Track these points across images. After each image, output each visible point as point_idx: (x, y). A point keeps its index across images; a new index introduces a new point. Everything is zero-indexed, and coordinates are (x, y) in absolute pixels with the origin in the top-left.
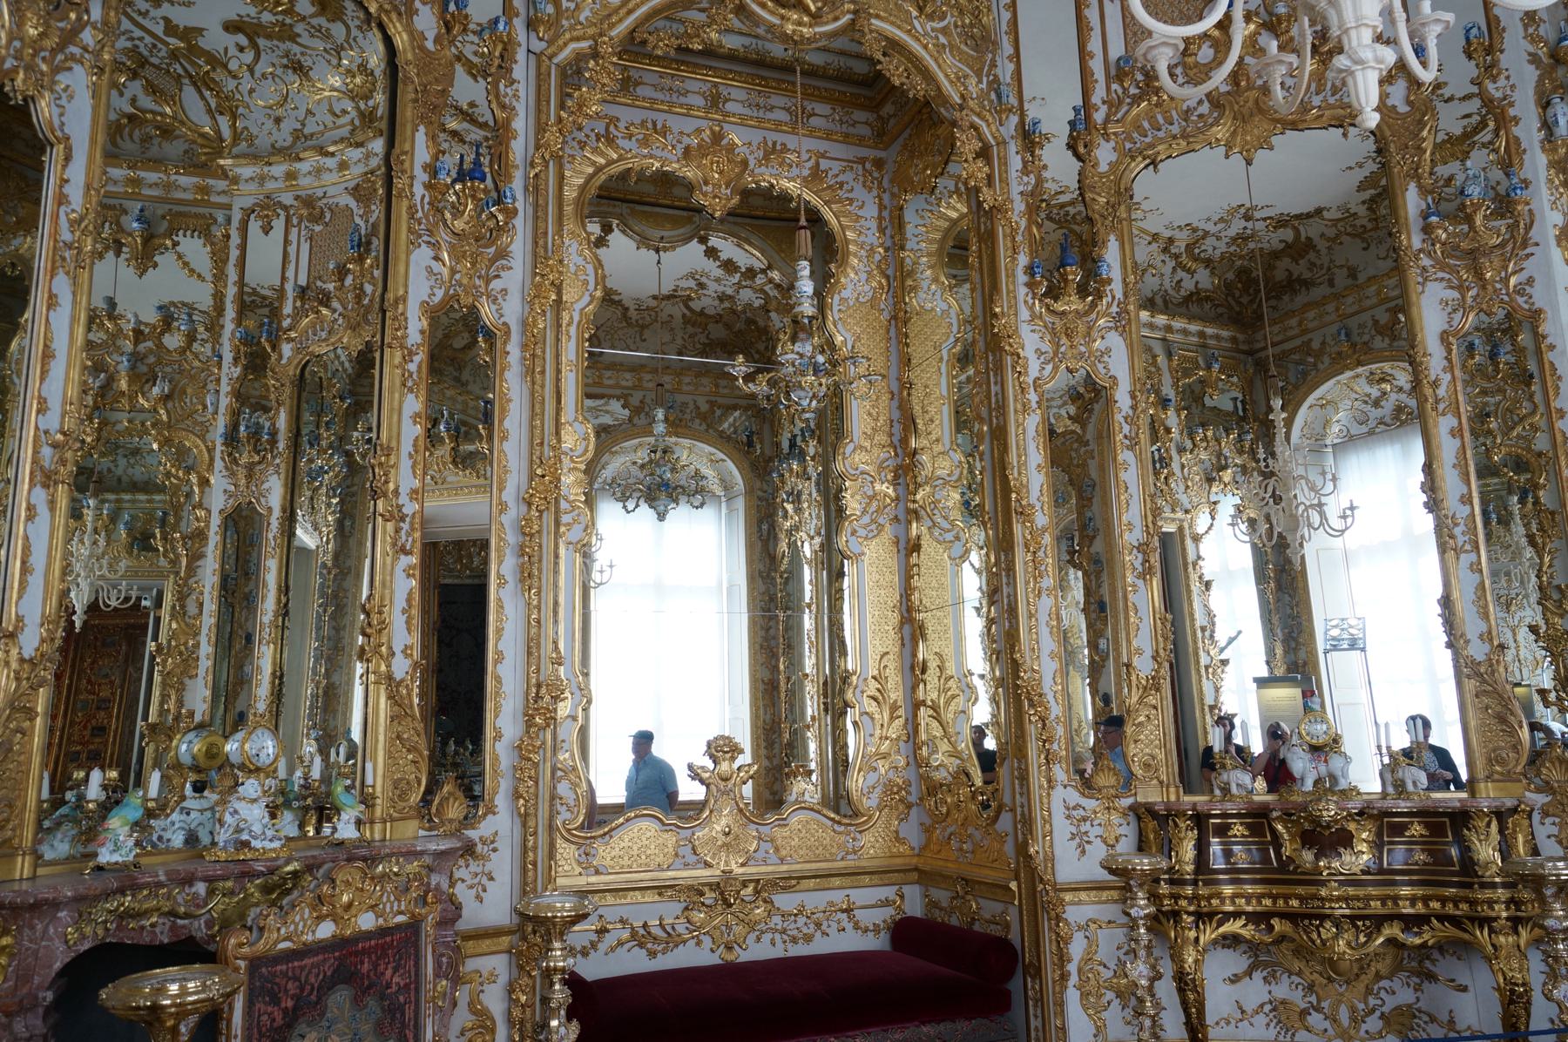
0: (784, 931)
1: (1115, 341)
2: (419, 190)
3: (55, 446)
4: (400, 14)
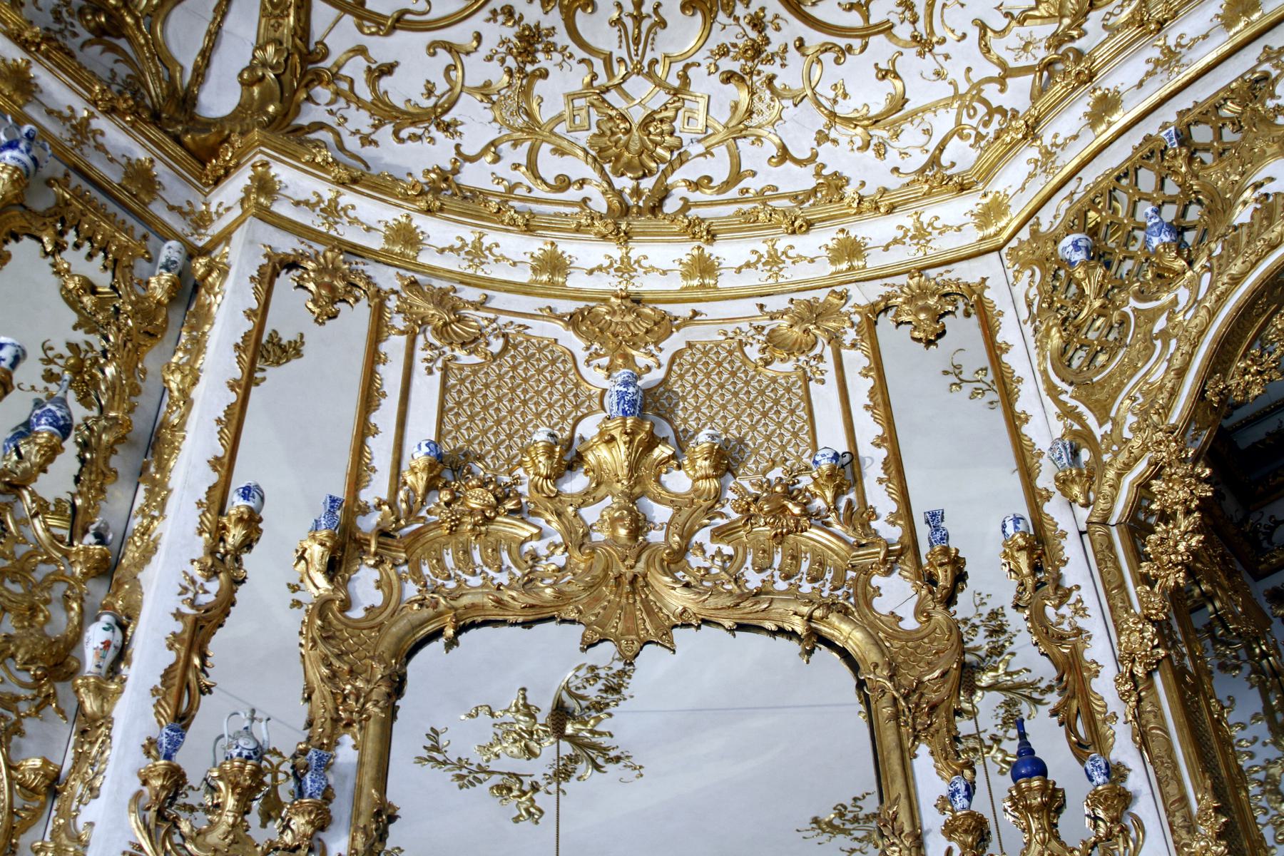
4: (845, 612)
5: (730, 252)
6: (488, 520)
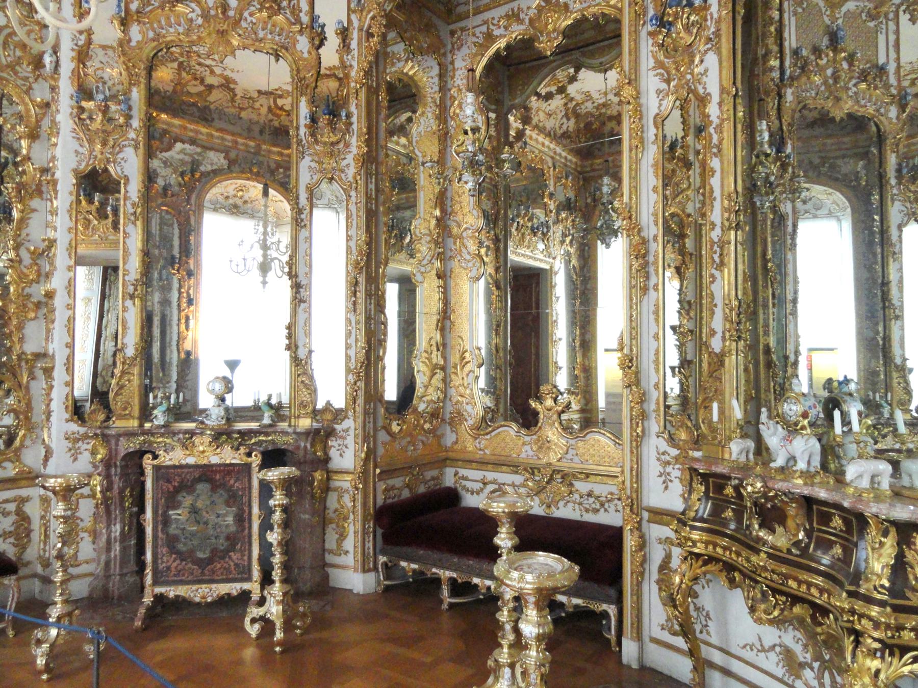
0: (580, 504)
1: (712, 60)
2: (303, 130)
3: (133, 285)
4: (287, 49)
6: (174, 6)
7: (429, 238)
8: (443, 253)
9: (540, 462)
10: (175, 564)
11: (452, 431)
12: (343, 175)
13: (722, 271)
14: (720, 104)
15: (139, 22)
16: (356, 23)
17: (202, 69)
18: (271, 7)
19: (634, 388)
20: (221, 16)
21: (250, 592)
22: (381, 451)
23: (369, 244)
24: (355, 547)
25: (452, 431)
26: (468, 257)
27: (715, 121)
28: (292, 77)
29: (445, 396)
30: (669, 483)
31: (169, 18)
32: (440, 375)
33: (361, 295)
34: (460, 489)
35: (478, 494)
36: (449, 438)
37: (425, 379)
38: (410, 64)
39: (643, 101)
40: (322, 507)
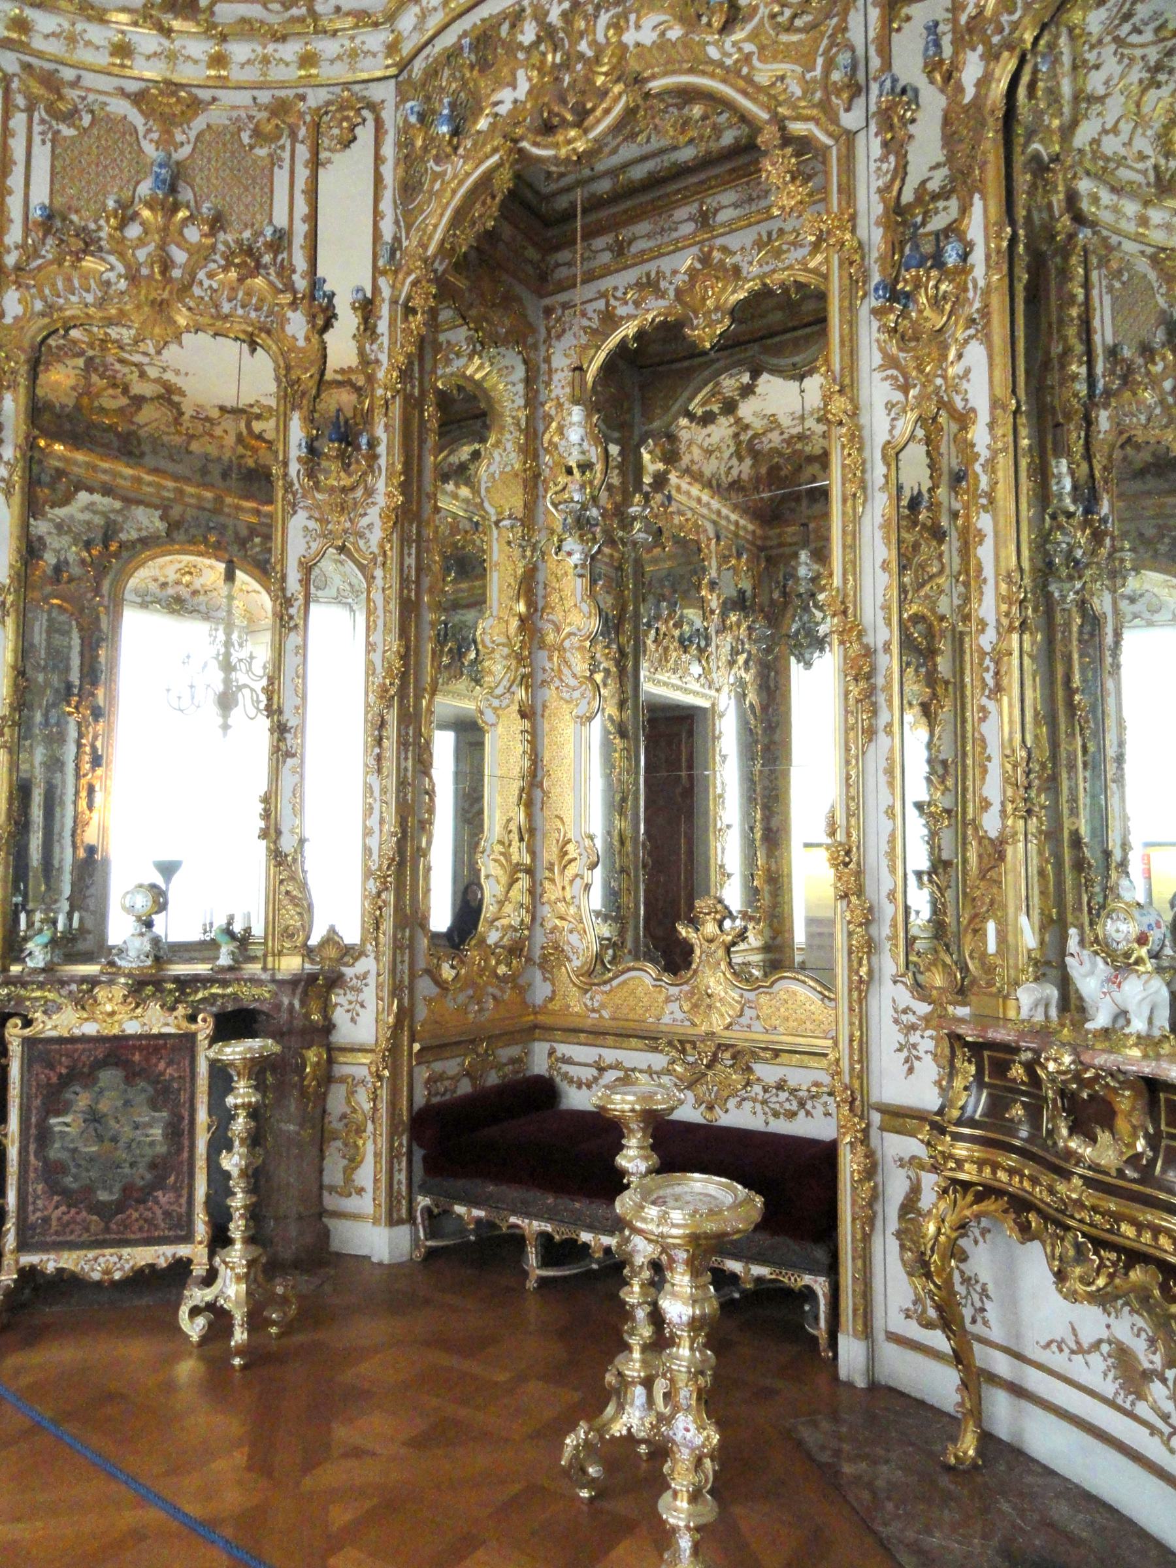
0: (764, 1102)
1: (976, 353)
2: (294, 468)
4: (269, 332)
5: (240, 51)
6: (79, 260)
7: (506, 651)
8: (530, 675)
9: (691, 1031)
10: (58, 1212)
11: (545, 979)
12: (361, 543)
13: (999, 701)
14: (991, 426)
15: (19, 286)
16: (386, 292)
17: (126, 370)
18: (244, 263)
19: (854, 899)
20: (158, 277)
21: (190, 1261)
22: (422, 1012)
23: (404, 657)
24: (376, 1181)
25: (545, 979)
26: (573, 682)
27: (984, 454)
28: (277, 379)
29: (533, 919)
30: (916, 1063)
31: (69, 280)
32: (524, 882)
33: (390, 744)
34: (558, 1079)
35: (589, 1087)
36: (541, 991)
37: (499, 890)
38: (477, 361)
39: (864, 420)
40: (319, 1111)
